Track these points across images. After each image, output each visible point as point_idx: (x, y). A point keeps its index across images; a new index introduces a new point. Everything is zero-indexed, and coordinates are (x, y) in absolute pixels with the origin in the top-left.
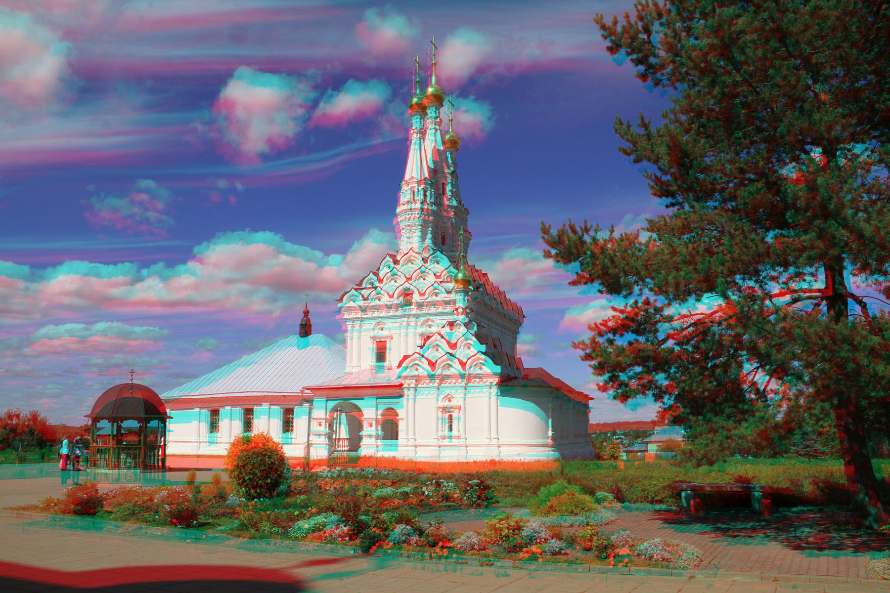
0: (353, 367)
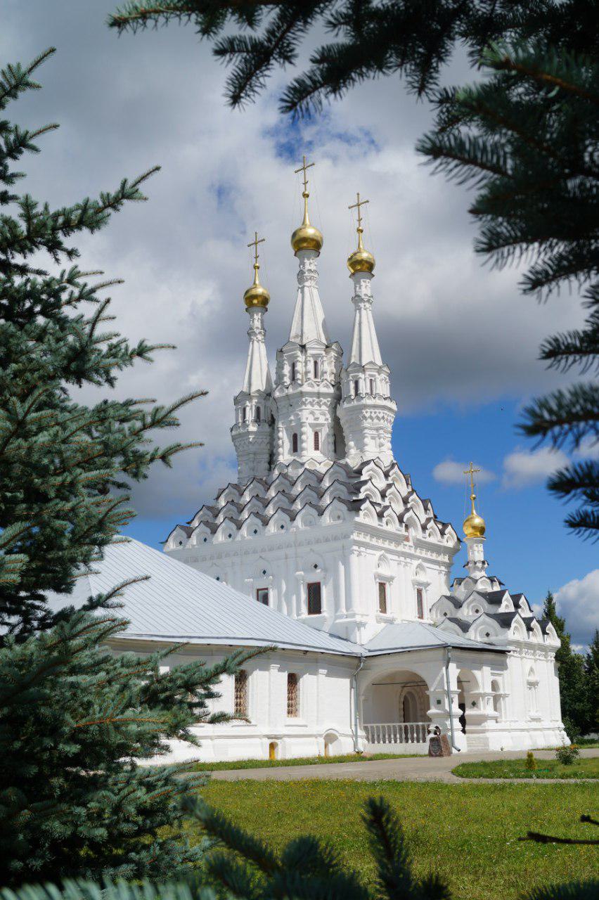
0: (362, 615)
